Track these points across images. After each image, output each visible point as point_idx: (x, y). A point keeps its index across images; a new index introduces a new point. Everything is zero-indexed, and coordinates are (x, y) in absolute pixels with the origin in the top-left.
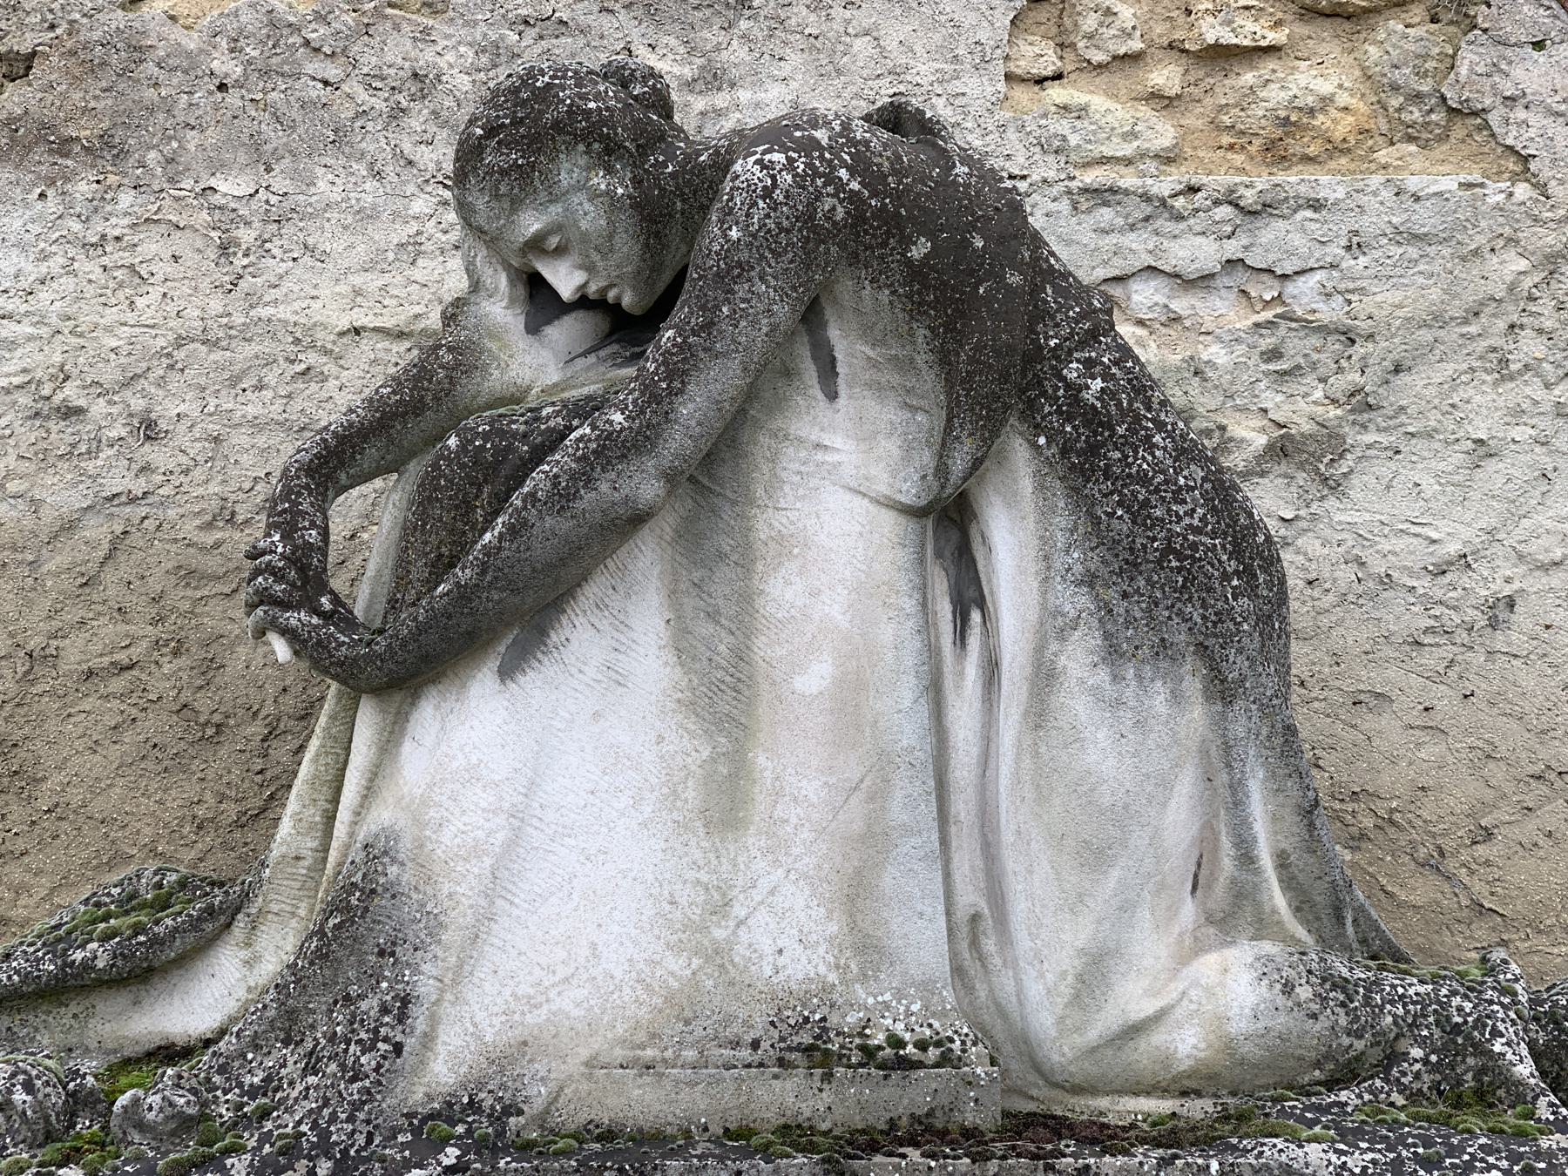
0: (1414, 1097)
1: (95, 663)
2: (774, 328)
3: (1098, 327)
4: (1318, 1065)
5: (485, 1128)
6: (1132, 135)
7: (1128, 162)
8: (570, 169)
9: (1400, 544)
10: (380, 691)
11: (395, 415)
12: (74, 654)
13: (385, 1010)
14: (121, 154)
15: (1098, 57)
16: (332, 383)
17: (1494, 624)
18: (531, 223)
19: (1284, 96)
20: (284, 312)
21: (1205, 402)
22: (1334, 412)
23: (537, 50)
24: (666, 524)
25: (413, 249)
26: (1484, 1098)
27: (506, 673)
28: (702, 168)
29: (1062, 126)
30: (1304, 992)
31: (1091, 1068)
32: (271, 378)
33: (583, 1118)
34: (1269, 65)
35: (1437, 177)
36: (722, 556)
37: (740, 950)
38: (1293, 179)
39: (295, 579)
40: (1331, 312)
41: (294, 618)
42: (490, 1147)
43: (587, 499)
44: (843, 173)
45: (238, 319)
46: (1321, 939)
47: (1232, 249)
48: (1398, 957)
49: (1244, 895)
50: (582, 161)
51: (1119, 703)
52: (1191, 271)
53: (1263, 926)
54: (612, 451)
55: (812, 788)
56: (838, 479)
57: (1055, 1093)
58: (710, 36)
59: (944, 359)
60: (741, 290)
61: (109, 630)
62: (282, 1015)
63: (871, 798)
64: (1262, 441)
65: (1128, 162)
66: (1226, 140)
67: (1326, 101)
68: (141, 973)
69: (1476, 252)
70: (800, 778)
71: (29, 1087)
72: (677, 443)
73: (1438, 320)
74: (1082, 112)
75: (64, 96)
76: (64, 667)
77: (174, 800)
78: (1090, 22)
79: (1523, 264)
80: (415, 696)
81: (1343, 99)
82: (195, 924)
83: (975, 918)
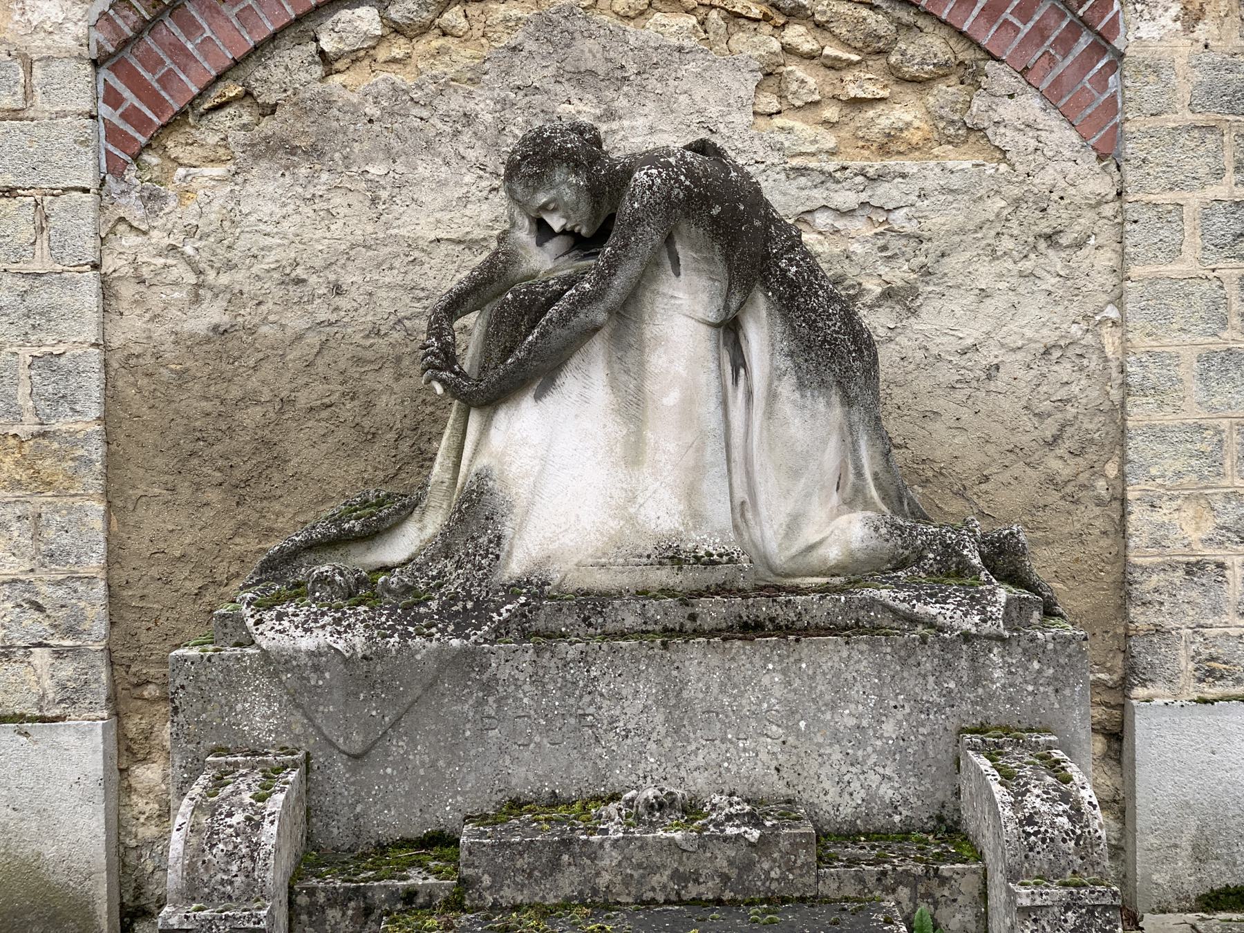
0: (930, 574)
1: (314, 404)
2: (653, 246)
3: (795, 242)
4: (889, 561)
5: (535, 590)
6: (816, 141)
7: (814, 154)
8: (559, 175)
9: (944, 339)
10: (480, 407)
11: (481, 285)
12: (304, 399)
13: (490, 541)
14: (322, 154)
15: (798, 103)
16: (426, 266)
17: (989, 378)
18: (542, 198)
19: (888, 122)
20: (403, 232)
21: (851, 271)
22: (913, 276)
23: (524, 101)
24: (605, 332)
25: (465, 200)
26: (959, 574)
27: (538, 397)
28: (618, 172)
29: (781, 137)
30: (883, 531)
31: (792, 566)
32: (397, 264)
33: (575, 587)
34: (881, 106)
35: (962, 161)
36: (630, 346)
37: (641, 518)
38: (892, 163)
39: (444, 358)
40: (911, 227)
41: (445, 375)
42: (539, 596)
43: (575, 321)
44: (682, 178)
45: (381, 235)
46: (894, 512)
47: (864, 197)
48: (926, 518)
49: (858, 490)
50: (565, 171)
51: (804, 407)
52: (844, 208)
53: (868, 505)
54: (585, 300)
55: (671, 447)
56: (681, 310)
57: (779, 579)
58: (609, 94)
59: (727, 258)
60: (639, 230)
61: (320, 388)
62: (444, 546)
63: (697, 451)
64: (879, 290)
65: (814, 154)
66: (861, 143)
67: (908, 124)
68: (373, 534)
69: (980, 198)
70: (666, 443)
71: (341, 574)
72: (613, 296)
73: (962, 231)
74: (790, 131)
75: (292, 125)
76: (298, 406)
77: (353, 469)
78: (794, 86)
79: (1003, 203)
80: (495, 410)
81: (917, 123)
82: (397, 512)
83: (743, 503)
